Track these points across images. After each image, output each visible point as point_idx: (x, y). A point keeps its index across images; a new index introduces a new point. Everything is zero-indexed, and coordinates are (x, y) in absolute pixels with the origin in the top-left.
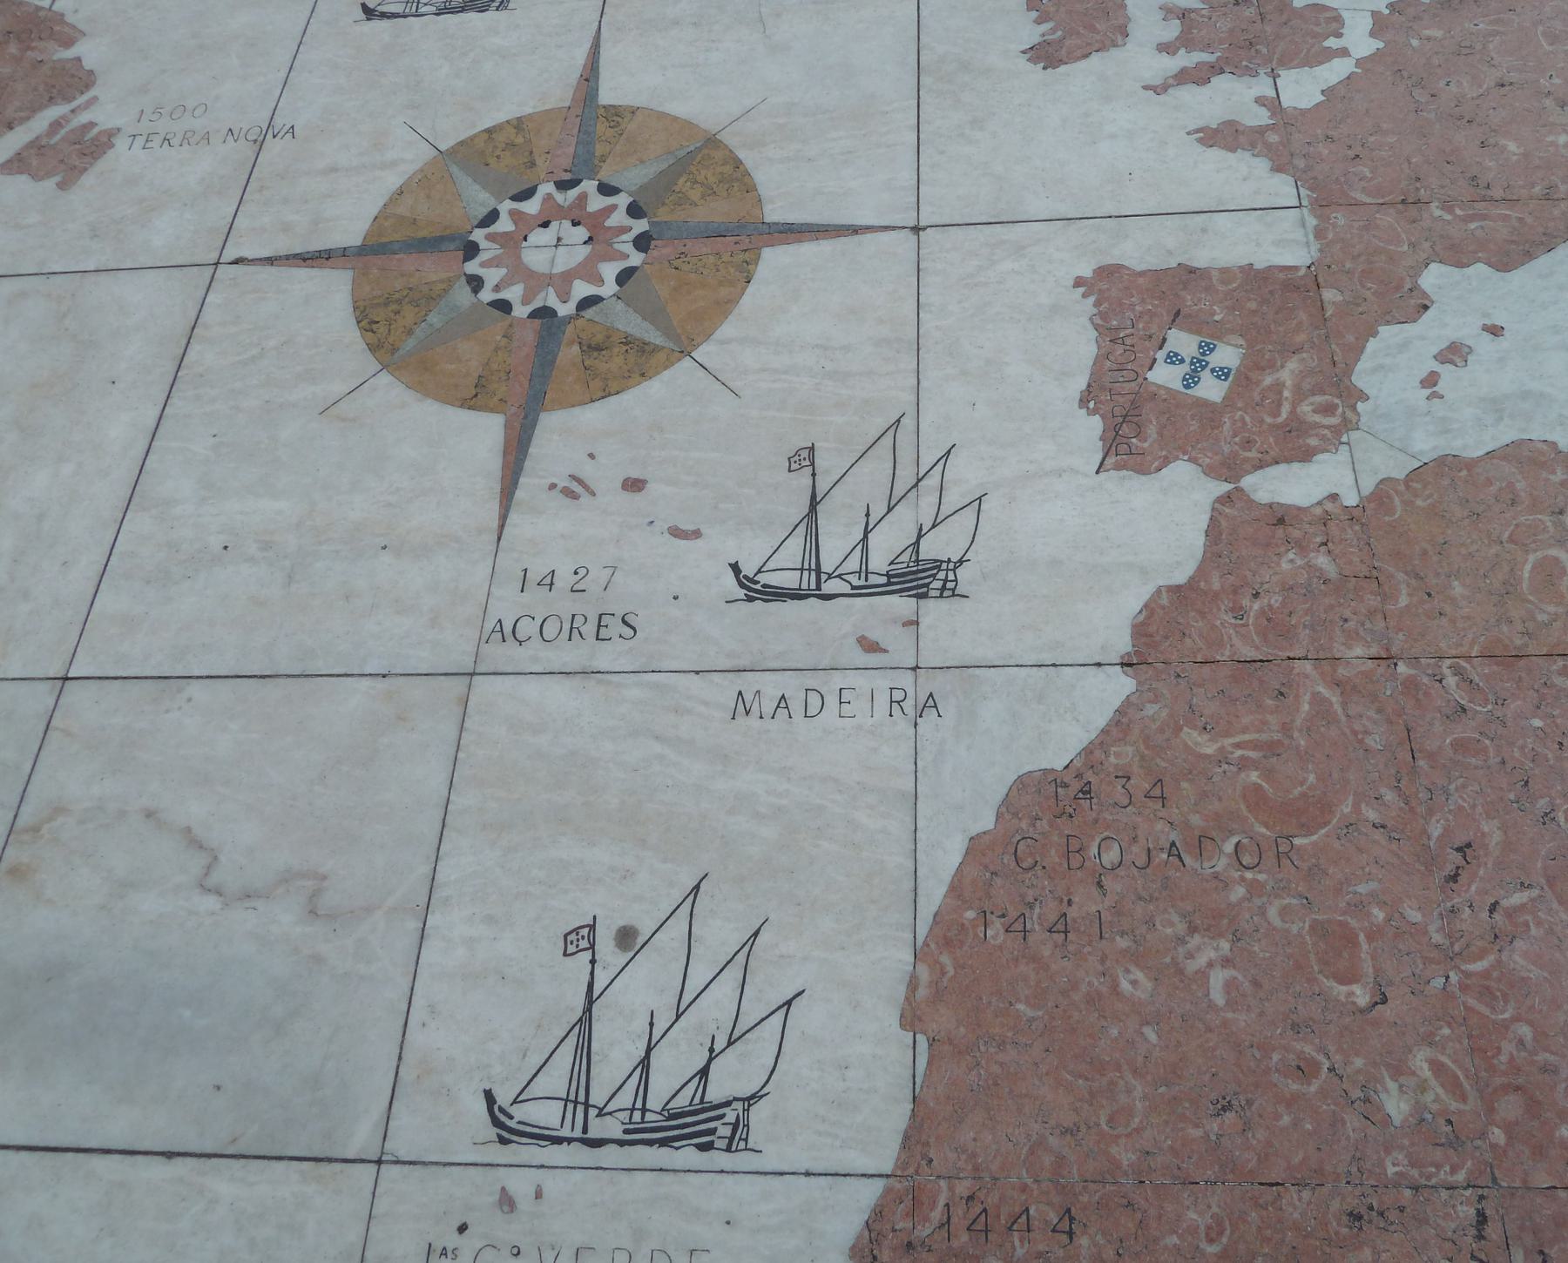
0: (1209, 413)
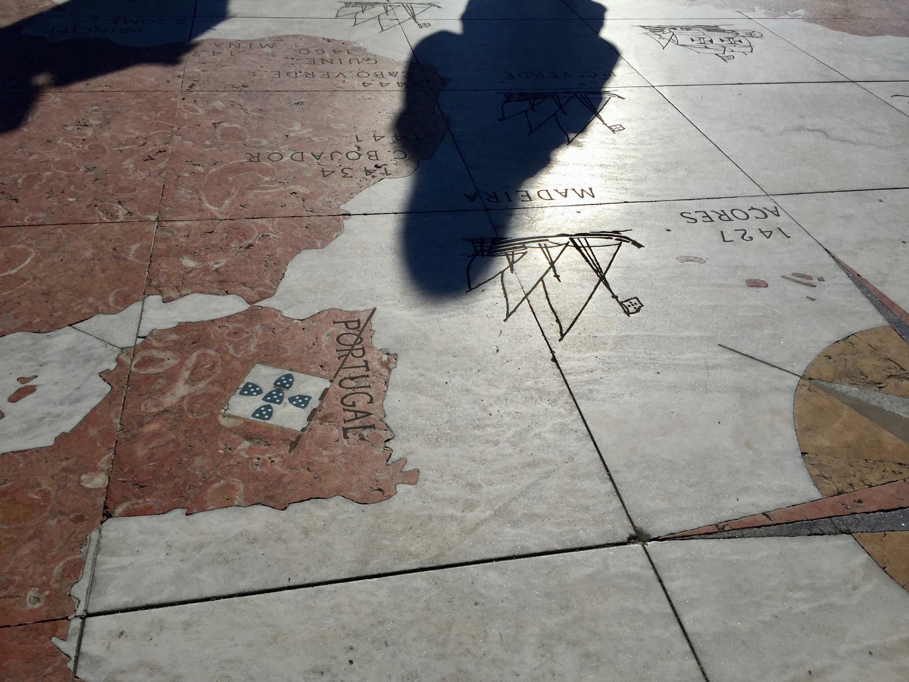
0: (270, 357)
